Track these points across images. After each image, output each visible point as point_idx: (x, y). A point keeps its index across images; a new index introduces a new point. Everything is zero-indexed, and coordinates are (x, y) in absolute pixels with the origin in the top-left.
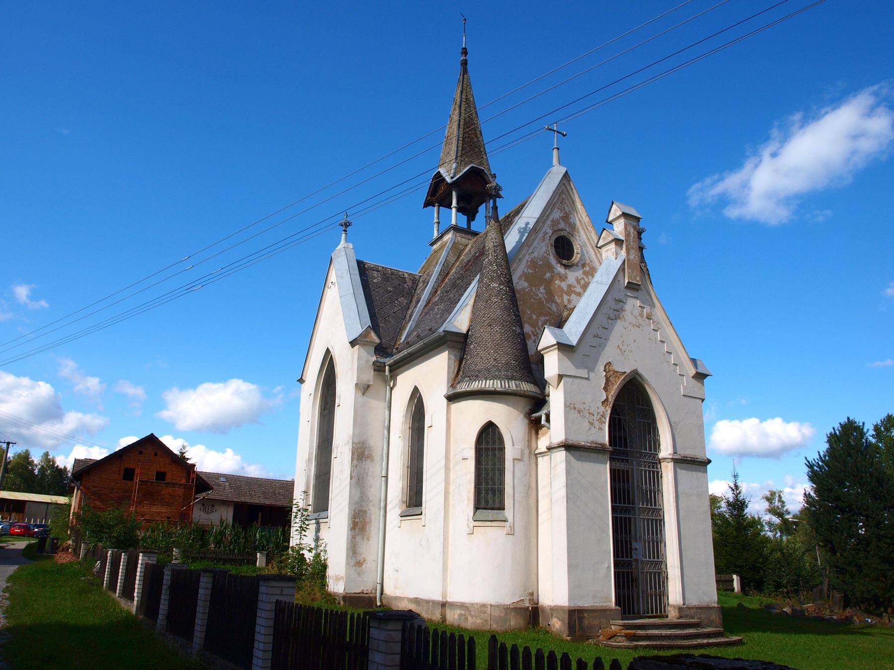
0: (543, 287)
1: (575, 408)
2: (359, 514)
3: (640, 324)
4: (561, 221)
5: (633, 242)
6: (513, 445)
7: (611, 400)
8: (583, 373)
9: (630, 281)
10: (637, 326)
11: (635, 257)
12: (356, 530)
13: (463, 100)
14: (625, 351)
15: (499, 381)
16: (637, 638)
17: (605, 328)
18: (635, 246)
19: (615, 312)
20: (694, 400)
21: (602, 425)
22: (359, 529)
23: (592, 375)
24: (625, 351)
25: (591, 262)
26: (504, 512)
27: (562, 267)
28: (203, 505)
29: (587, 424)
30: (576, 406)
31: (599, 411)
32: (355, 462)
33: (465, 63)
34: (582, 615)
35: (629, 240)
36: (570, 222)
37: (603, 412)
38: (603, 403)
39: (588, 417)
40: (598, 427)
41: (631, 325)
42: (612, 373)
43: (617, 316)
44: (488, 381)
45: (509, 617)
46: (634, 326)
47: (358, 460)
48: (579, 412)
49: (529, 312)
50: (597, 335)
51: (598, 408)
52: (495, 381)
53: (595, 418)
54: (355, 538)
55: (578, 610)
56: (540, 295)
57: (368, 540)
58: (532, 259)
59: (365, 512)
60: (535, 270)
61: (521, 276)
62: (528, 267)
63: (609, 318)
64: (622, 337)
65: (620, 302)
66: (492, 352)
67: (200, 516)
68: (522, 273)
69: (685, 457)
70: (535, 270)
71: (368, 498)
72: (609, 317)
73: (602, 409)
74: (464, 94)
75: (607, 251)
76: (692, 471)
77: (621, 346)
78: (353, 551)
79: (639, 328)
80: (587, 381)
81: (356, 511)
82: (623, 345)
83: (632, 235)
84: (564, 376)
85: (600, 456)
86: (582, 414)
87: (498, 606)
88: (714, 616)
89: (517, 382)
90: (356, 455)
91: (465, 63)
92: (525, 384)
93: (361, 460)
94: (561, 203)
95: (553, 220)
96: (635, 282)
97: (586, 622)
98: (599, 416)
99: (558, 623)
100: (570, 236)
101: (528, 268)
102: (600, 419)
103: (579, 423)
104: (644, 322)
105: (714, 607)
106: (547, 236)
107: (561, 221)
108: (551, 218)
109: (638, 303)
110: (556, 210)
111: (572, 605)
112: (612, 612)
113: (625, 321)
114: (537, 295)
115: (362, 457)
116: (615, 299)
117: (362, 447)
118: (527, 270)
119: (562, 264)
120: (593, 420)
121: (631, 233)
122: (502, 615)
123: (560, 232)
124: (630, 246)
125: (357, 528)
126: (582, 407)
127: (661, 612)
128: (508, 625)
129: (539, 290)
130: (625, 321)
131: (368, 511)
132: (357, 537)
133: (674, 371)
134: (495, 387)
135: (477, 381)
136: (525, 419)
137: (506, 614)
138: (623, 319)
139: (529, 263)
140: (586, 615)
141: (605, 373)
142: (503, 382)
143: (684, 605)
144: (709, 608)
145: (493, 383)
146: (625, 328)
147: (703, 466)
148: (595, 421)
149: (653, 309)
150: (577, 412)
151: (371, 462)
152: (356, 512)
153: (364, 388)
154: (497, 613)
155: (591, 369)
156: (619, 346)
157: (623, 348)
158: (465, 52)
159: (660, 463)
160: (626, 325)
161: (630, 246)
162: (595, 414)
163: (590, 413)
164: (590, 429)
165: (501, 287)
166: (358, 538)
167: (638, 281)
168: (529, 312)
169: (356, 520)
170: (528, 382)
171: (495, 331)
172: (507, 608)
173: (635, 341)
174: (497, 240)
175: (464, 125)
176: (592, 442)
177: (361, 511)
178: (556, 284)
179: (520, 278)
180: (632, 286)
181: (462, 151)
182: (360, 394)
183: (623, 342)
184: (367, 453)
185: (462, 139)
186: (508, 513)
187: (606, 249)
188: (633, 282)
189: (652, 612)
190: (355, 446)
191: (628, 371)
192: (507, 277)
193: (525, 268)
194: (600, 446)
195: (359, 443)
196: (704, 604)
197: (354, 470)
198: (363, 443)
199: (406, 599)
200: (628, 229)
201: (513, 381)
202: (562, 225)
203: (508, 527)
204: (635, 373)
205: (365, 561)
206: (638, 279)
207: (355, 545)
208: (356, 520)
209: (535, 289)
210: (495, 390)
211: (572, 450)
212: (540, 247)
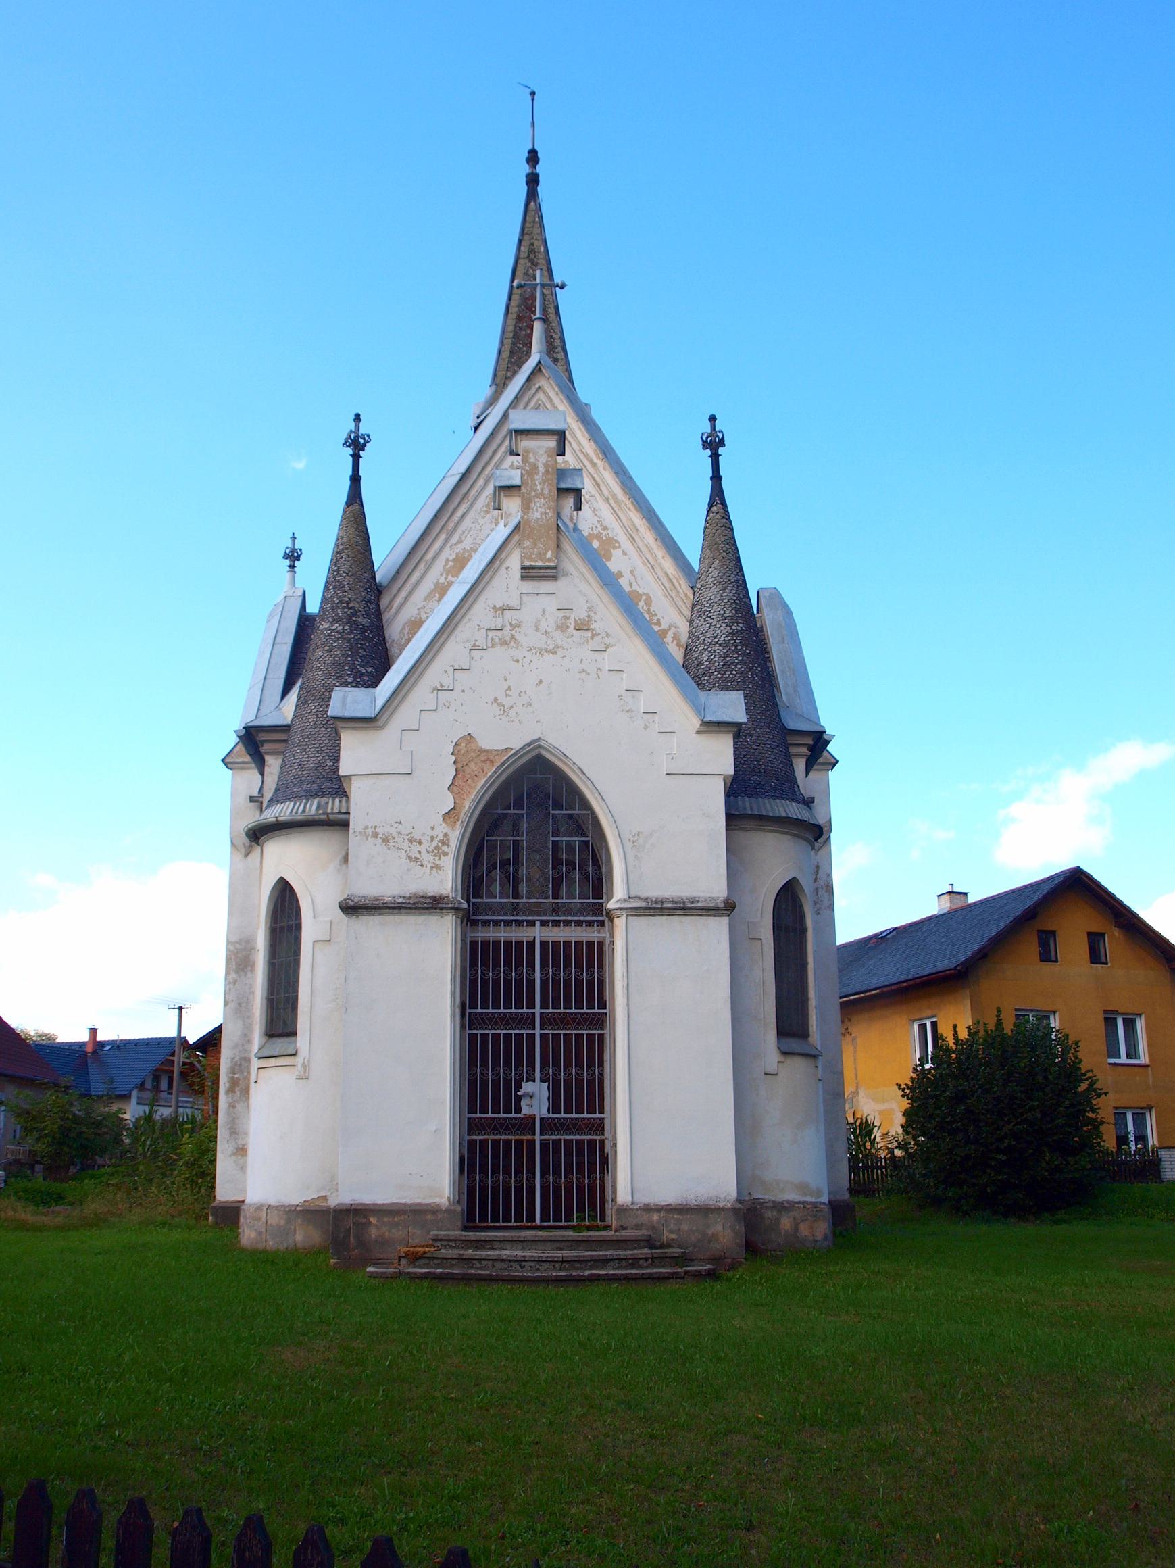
1: (375, 835)
2: (240, 1065)
3: (557, 647)
5: (543, 482)
6: (314, 917)
7: (467, 805)
9: (527, 563)
10: (546, 651)
11: (546, 513)
12: (235, 1092)
13: (522, 255)
14: (512, 707)
16: (436, 1261)
17: (462, 669)
18: (546, 491)
19: (491, 634)
21: (439, 859)
22: (241, 1091)
24: (512, 707)
25: (605, 528)
26: (295, 1042)
29: (404, 861)
31: (434, 833)
32: (233, 975)
33: (533, 181)
34: (364, 1220)
35: (533, 480)
38: (446, 816)
40: (429, 866)
41: (534, 651)
45: (293, 1227)
46: (540, 652)
47: (237, 972)
48: (386, 840)
50: (442, 686)
51: (433, 828)
54: (234, 1107)
58: (457, 554)
63: (474, 648)
64: (506, 680)
65: (505, 612)
68: (433, 587)
69: (656, 902)
72: (474, 645)
74: (526, 243)
77: (502, 699)
78: (230, 1129)
79: (555, 653)
81: (235, 1060)
82: (507, 695)
83: (541, 469)
84: (353, 777)
86: (391, 844)
87: (277, 1208)
88: (720, 1228)
89: (324, 800)
90: (234, 963)
91: (533, 181)
92: (340, 801)
96: (540, 564)
97: (374, 1233)
98: (435, 843)
101: (447, 575)
102: (437, 848)
112: (440, 1216)
115: (246, 966)
117: (245, 949)
118: (446, 578)
120: (420, 852)
122: (282, 1222)
124: (533, 494)
125: (237, 1089)
126: (393, 831)
127: (603, 1219)
128: (291, 1241)
130: (517, 648)
133: (646, 727)
137: (288, 1221)
138: (512, 644)
139: (451, 564)
140: (373, 1220)
141: (453, 758)
142: (298, 804)
143: (632, 1203)
144: (705, 1211)
146: (517, 661)
147: (715, 916)
152: (236, 1063)
153: (244, 844)
154: (274, 1220)
156: (496, 700)
157: (507, 702)
158: (533, 158)
159: (612, 921)
160: (518, 654)
161: (533, 494)
162: (426, 839)
163: (411, 841)
164: (408, 870)
165: (334, 627)
167: (550, 560)
169: (236, 1076)
172: (290, 1211)
173: (541, 682)
174: (345, 540)
182: (239, 856)
183: (509, 688)
185: (511, 335)
186: (302, 1041)
188: (533, 564)
190: (232, 948)
191: (516, 744)
192: (350, 605)
193: (441, 575)
194: (429, 900)
195: (239, 942)
197: (230, 989)
200: (532, 460)
203: (299, 1065)
204: (535, 745)
206: (549, 554)
207: (234, 1119)
208: (236, 1076)
211: (363, 915)
212: (478, 527)
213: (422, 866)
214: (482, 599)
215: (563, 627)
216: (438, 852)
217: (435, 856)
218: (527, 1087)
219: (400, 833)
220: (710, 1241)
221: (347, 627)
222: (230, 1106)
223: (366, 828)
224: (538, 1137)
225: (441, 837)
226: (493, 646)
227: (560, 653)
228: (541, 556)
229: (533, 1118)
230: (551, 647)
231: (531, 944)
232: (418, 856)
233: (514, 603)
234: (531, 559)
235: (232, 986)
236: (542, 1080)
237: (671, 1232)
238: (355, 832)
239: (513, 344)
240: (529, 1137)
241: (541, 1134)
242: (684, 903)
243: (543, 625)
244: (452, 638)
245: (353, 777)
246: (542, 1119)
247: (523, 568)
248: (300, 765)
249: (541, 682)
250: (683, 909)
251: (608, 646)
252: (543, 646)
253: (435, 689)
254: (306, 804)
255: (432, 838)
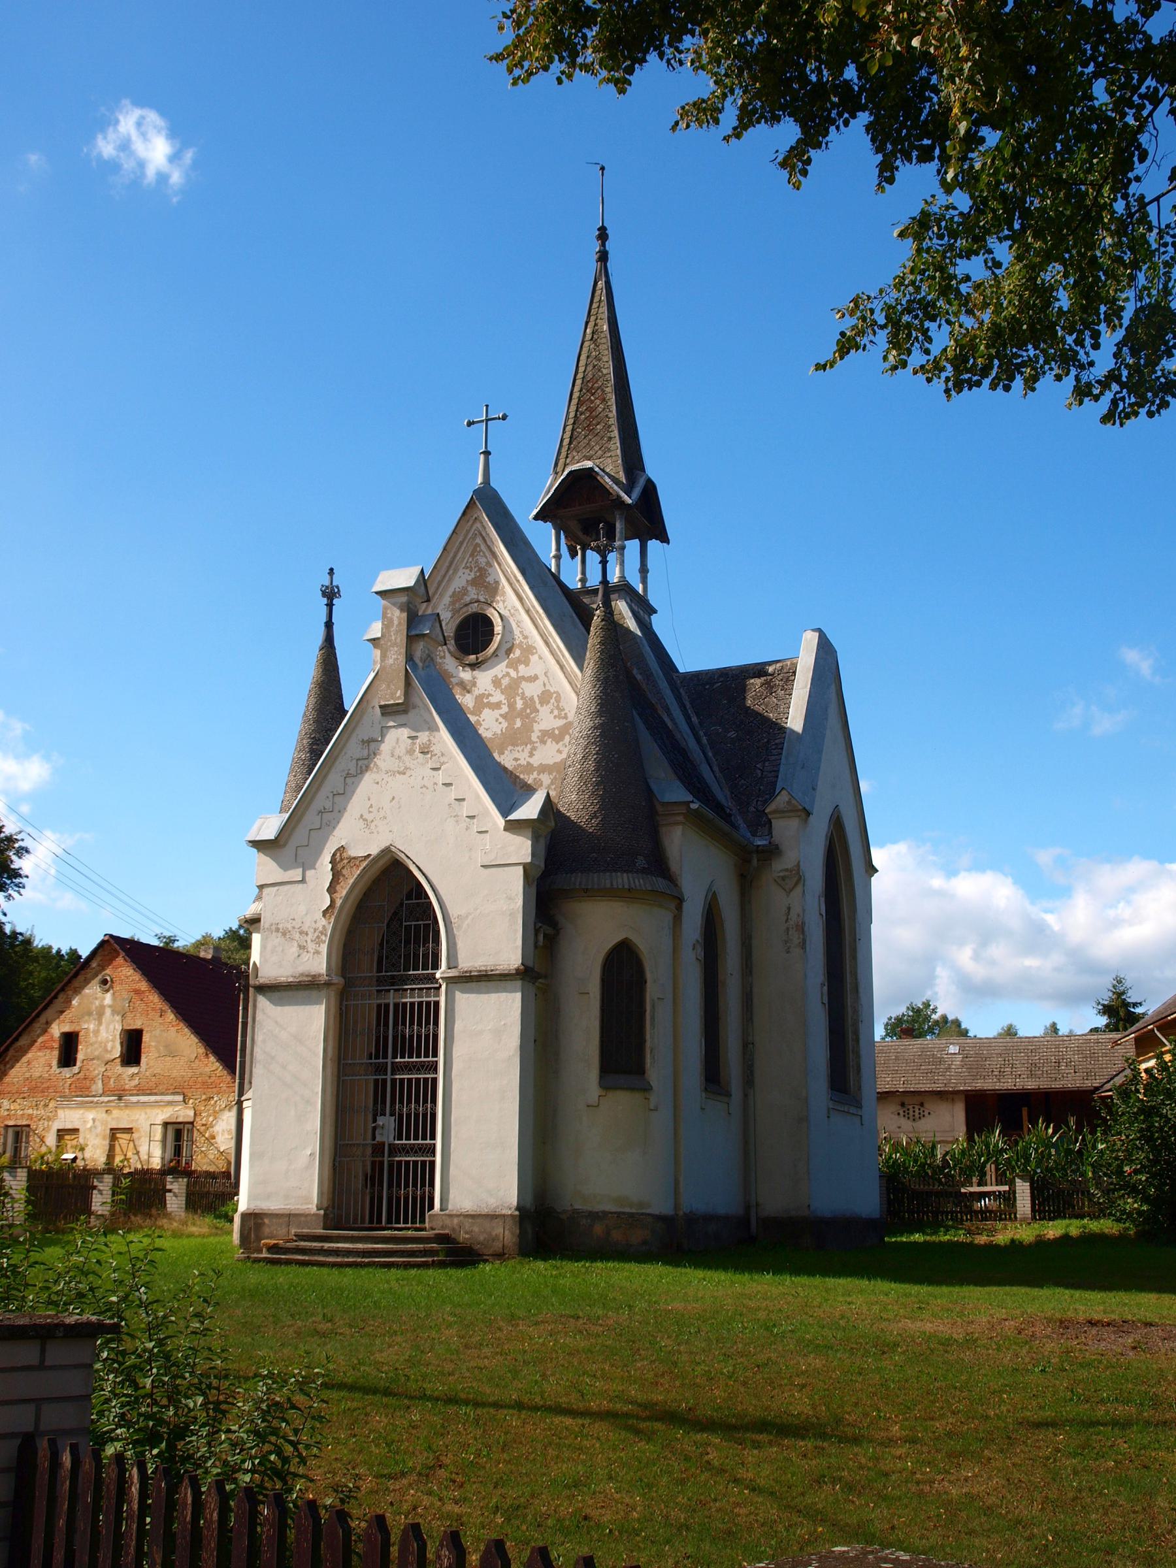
1: (277, 930)
3: (406, 768)
4: (469, 588)
5: (397, 632)
7: (339, 902)
8: (296, 874)
10: (399, 773)
13: (587, 339)
18: (398, 640)
19: (360, 763)
20: (506, 869)
23: (309, 873)
25: (526, 637)
27: (467, 669)
28: (903, 1105)
29: (294, 949)
30: (280, 926)
33: (603, 257)
34: (260, 1221)
36: (489, 583)
37: (324, 926)
38: (325, 913)
39: (297, 938)
42: (345, 861)
43: (364, 768)
48: (284, 934)
51: (315, 922)
53: (309, 939)
55: (256, 1214)
63: (348, 775)
67: (899, 1127)
69: (466, 972)
73: (324, 922)
74: (591, 324)
76: (488, 992)
79: (404, 774)
80: (300, 886)
83: (396, 622)
85: (314, 993)
91: (603, 257)
94: (472, 555)
95: (454, 592)
100: (485, 607)
102: (318, 937)
103: (283, 950)
104: (415, 762)
105: (504, 1216)
108: (450, 591)
109: (404, 732)
110: (460, 573)
111: (252, 1207)
112: (309, 1218)
119: (464, 665)
121: (395, 618)
123: (465, 609)
126: (289, 926)
140: (266, 1221)
146: (378, 783)
148: (309, 941)
149: (436, 733)
155: (307, 863)
156: (362, 816)
157: (369, 817)
158: (603, 235)
163: (301, 933)
167: (399, 698)
173: (393, 798)
175: (581, 391)
176: (302, 975)
181: (570, 443)
183: (371, 806)
189: (363, 1221)
191: (374, 851)
196: (485, 1211)
202: (473, 594)
204: (387, 851)
214: (354, 735)
215: (410, 752)
216: (318, 941)
218: (381, 1121)
219: (294, 928)
220: (493, 1241)
223: (272, 925)
224: (386, 1159)
225: (321, 929)
227: (408, 774)
228: (393, 696)
229: (383, 1144)
231: (387, 1006)
236: (391, 1115)
237: (466, 1233)
239: (573, 430)
240: (381, 1159)
241: (389, 1156)
243: (397, 753)
244: (333, 770)
246: (390, 1145)
249: (393, 798)
251: (442, 764)
252: (396, 769)
253: (320, 812)
255: (315, 930)
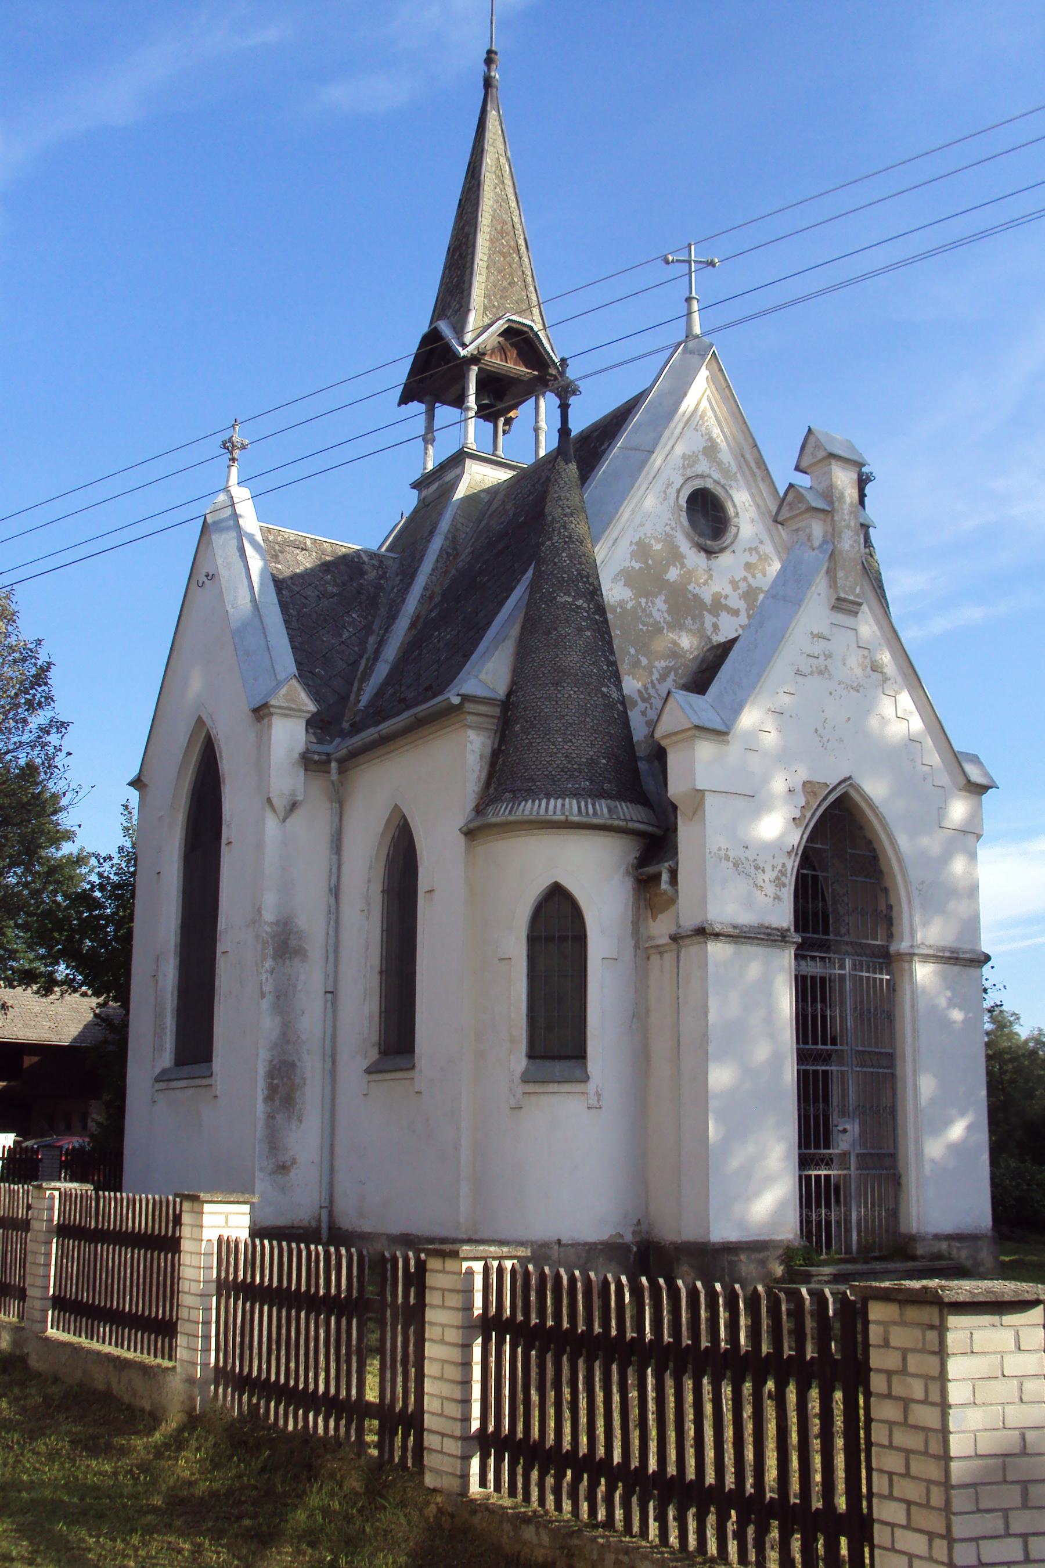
0: (663, 598)
1: (727, 858)
3: (859, 685)
4: (701, 456)
15: (574, 802)
30: (730, 854)
34: (736, 1259)
44: (552, 801)
47: (274, 958)
49: (632, 651)
52: (567, 800)
54: (273, 1118)
56: (655, 613)
57: (300, 1121)
59: (292, 1065)
60: (646, 563)
61: (617, 575)
62: (633, 555)
63: (799, 673)
66: (560, 740)
70: (646, 563)
71: (299, 1037)
72: (798, 670)
75: (797, 530)
79: (858, 691)
84: (706, 793)
90: (271, 948)
93: (281, 958)
96: (851, 598)
98: (775, 873)
99: (689, 1275)
102: (777, 878)
106: (672, 491)
107: (701, 456)
113: (830, 679)
114: (651, 615)
116: (812, 633)
129: (653, 603)
130: (830, 679)
131: (298, 1064)
132: (278, 1116)
134: (567, 813)
135: (530, 802)
136: (627, 879)
138: (826, 674)
142: (583, 804)
145: (563, 805)
150: (731, 865)
151: (303, 961)
161: (843, 523)
163: (757, 868)
166: (280, 1118)
167: (858, 596)
168: (632, 651)
169: (276, 1082)
170: (631, 802)
171: (566, 696)
173: (849, 719)
177: (284, 1062)
178: (690, 591)
179: (615, 580)
180: (845, 606)
184: (293, 943)
187: (795, 527)
197: (267, 979)
198: (286, 924)
199: (385, 1237)
201: (603, 801)
202: (702, 466)
205: (294, 1162)
206: (858, 590)
208: (276, 1082)
209: (647, 603)
210: (567, 820)
213: (766, 895)
217: (776, 886)
219: (747, 859)
221: (591, 606)
222: (269, 1117)
223: (720, 849)
225: (780, 867)
226: (812, 674)
230: (855, 685)
232: (762, 885)
233: (826, 632)
234: (845, 592)
235: (269, 975)
238: (710, 852)
242: (958, 953)
245: (706, 793)
247: (838, 599)
248: (566, 757)
250: (957, 959)
254: (594, 805)
255: (773, 866)
